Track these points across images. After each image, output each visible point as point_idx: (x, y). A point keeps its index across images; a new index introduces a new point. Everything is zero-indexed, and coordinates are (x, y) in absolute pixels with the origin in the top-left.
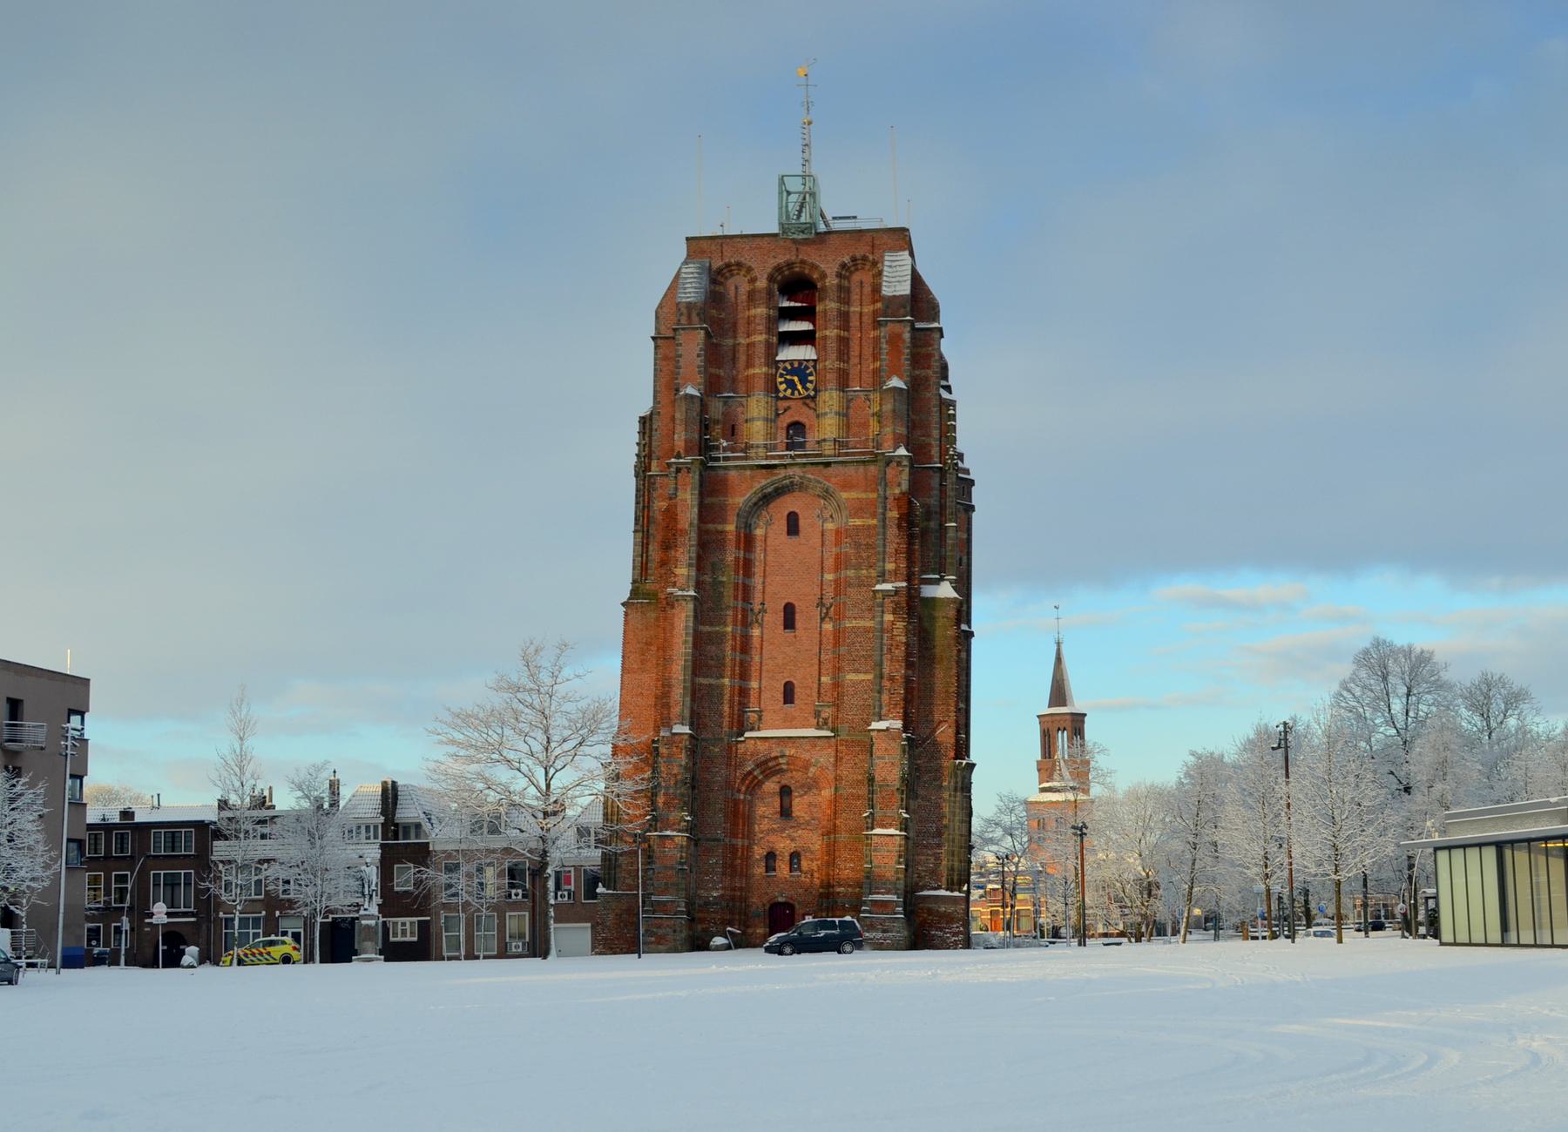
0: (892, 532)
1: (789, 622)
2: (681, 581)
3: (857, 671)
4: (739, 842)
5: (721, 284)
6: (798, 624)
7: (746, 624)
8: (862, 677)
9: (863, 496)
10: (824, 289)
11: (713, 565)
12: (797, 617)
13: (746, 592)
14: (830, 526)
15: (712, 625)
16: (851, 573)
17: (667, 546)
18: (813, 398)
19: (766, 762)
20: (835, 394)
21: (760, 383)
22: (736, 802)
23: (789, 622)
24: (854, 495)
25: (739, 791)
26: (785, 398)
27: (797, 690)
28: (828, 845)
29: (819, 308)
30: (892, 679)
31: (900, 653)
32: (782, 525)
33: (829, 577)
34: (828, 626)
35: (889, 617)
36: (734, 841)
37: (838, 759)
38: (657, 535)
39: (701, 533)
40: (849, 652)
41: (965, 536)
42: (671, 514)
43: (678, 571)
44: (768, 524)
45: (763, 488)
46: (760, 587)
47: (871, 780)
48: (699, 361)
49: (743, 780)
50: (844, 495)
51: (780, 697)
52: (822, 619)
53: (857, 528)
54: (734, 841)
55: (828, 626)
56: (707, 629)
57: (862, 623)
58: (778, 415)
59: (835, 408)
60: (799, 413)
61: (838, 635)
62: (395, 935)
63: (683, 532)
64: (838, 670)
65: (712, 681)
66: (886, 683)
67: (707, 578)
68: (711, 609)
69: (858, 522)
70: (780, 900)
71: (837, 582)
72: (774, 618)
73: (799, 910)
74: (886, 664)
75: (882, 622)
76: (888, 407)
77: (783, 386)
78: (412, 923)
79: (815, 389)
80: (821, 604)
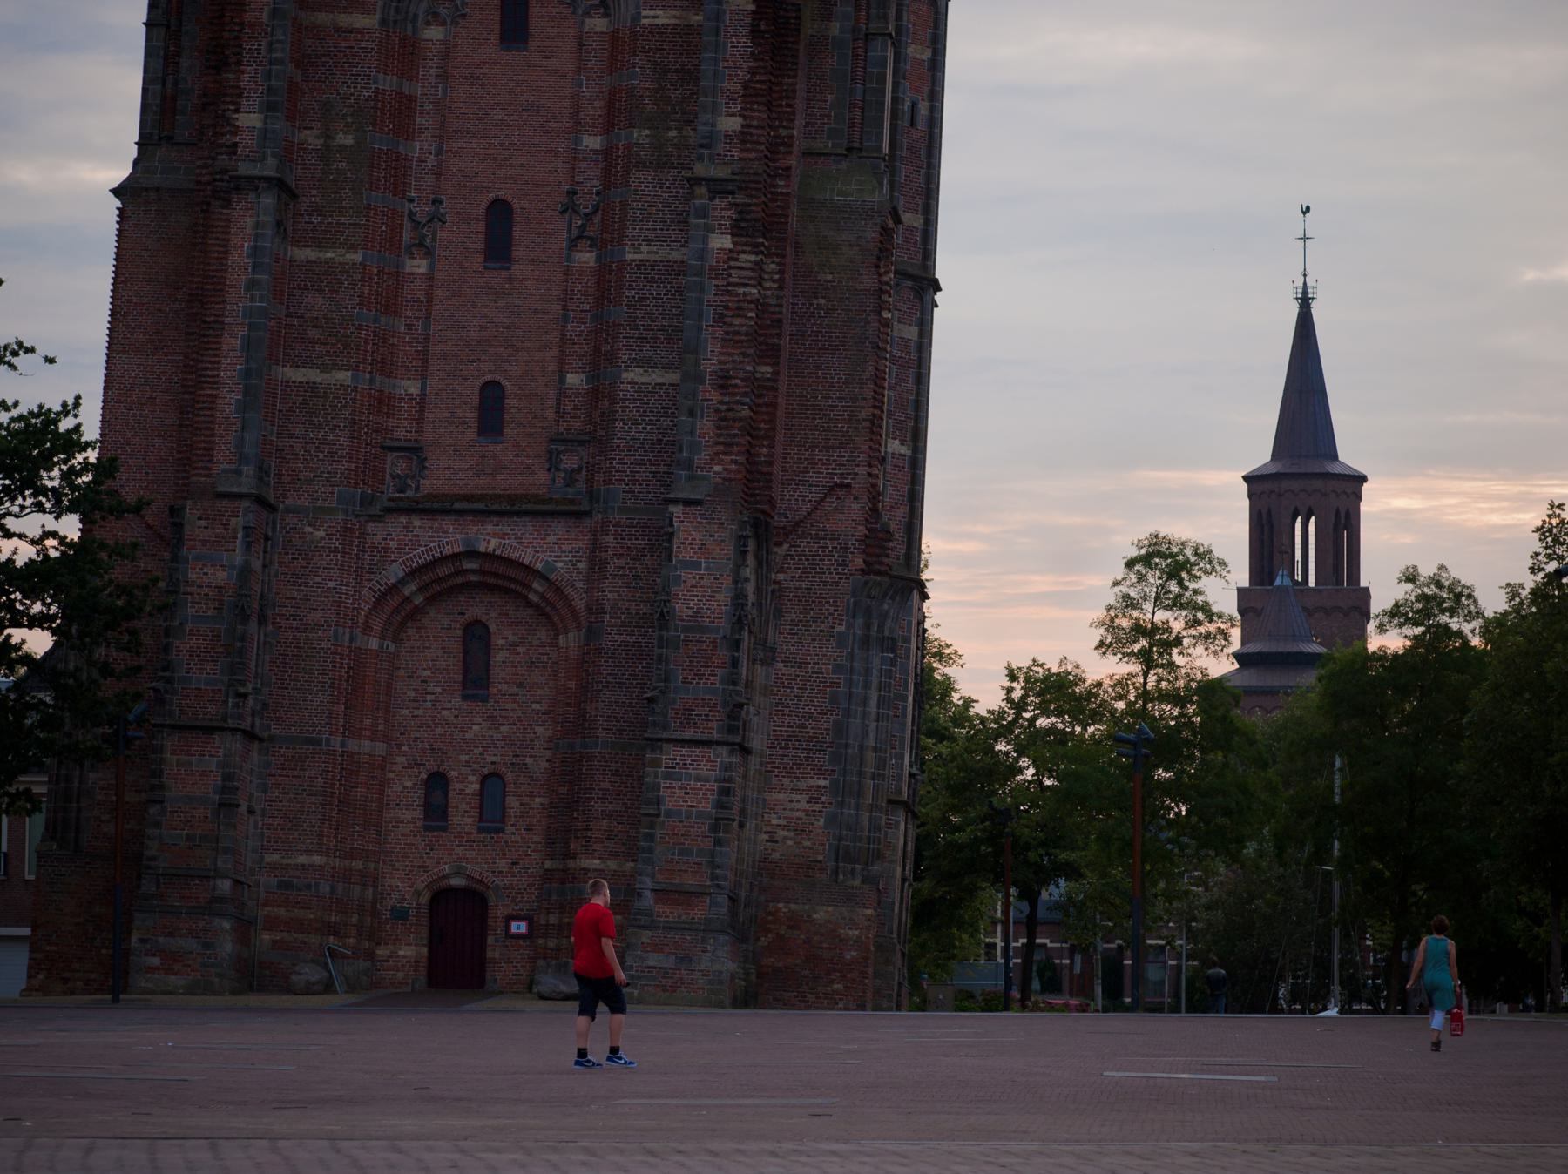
0: (738, 43)
1: (498, 248)
2: (247, 142)
3: (648, 364)
4: (363, 747)
6: (519, 251)
8: (657, 377)
12: (517, 232)
14: (599, 24)
15: (320, 246)
16: (641, 135)
23: (498, 248)
25: (367, 629)
27: (511, 403)
30: (723, 384)
33: (592, 142)
34: (586, 258)
35: (726, 242)
36: (352, 745)
37: (597, 566)
41: (927, 55)
46: (431, 161)
49: (379, 602)
51: (470, 416)
52: (573, 244)
53: (658, 31)
54: (352, 745)
55: (586, 258)
56: (310, 254)
61: (607, 279)
64: (601, 363)
65: (314, 376)
67: (312, 138)
70: (457, 882)
71: (608, 153)
73: (498, 909)
75: (702, 254)
80: (569, 208)
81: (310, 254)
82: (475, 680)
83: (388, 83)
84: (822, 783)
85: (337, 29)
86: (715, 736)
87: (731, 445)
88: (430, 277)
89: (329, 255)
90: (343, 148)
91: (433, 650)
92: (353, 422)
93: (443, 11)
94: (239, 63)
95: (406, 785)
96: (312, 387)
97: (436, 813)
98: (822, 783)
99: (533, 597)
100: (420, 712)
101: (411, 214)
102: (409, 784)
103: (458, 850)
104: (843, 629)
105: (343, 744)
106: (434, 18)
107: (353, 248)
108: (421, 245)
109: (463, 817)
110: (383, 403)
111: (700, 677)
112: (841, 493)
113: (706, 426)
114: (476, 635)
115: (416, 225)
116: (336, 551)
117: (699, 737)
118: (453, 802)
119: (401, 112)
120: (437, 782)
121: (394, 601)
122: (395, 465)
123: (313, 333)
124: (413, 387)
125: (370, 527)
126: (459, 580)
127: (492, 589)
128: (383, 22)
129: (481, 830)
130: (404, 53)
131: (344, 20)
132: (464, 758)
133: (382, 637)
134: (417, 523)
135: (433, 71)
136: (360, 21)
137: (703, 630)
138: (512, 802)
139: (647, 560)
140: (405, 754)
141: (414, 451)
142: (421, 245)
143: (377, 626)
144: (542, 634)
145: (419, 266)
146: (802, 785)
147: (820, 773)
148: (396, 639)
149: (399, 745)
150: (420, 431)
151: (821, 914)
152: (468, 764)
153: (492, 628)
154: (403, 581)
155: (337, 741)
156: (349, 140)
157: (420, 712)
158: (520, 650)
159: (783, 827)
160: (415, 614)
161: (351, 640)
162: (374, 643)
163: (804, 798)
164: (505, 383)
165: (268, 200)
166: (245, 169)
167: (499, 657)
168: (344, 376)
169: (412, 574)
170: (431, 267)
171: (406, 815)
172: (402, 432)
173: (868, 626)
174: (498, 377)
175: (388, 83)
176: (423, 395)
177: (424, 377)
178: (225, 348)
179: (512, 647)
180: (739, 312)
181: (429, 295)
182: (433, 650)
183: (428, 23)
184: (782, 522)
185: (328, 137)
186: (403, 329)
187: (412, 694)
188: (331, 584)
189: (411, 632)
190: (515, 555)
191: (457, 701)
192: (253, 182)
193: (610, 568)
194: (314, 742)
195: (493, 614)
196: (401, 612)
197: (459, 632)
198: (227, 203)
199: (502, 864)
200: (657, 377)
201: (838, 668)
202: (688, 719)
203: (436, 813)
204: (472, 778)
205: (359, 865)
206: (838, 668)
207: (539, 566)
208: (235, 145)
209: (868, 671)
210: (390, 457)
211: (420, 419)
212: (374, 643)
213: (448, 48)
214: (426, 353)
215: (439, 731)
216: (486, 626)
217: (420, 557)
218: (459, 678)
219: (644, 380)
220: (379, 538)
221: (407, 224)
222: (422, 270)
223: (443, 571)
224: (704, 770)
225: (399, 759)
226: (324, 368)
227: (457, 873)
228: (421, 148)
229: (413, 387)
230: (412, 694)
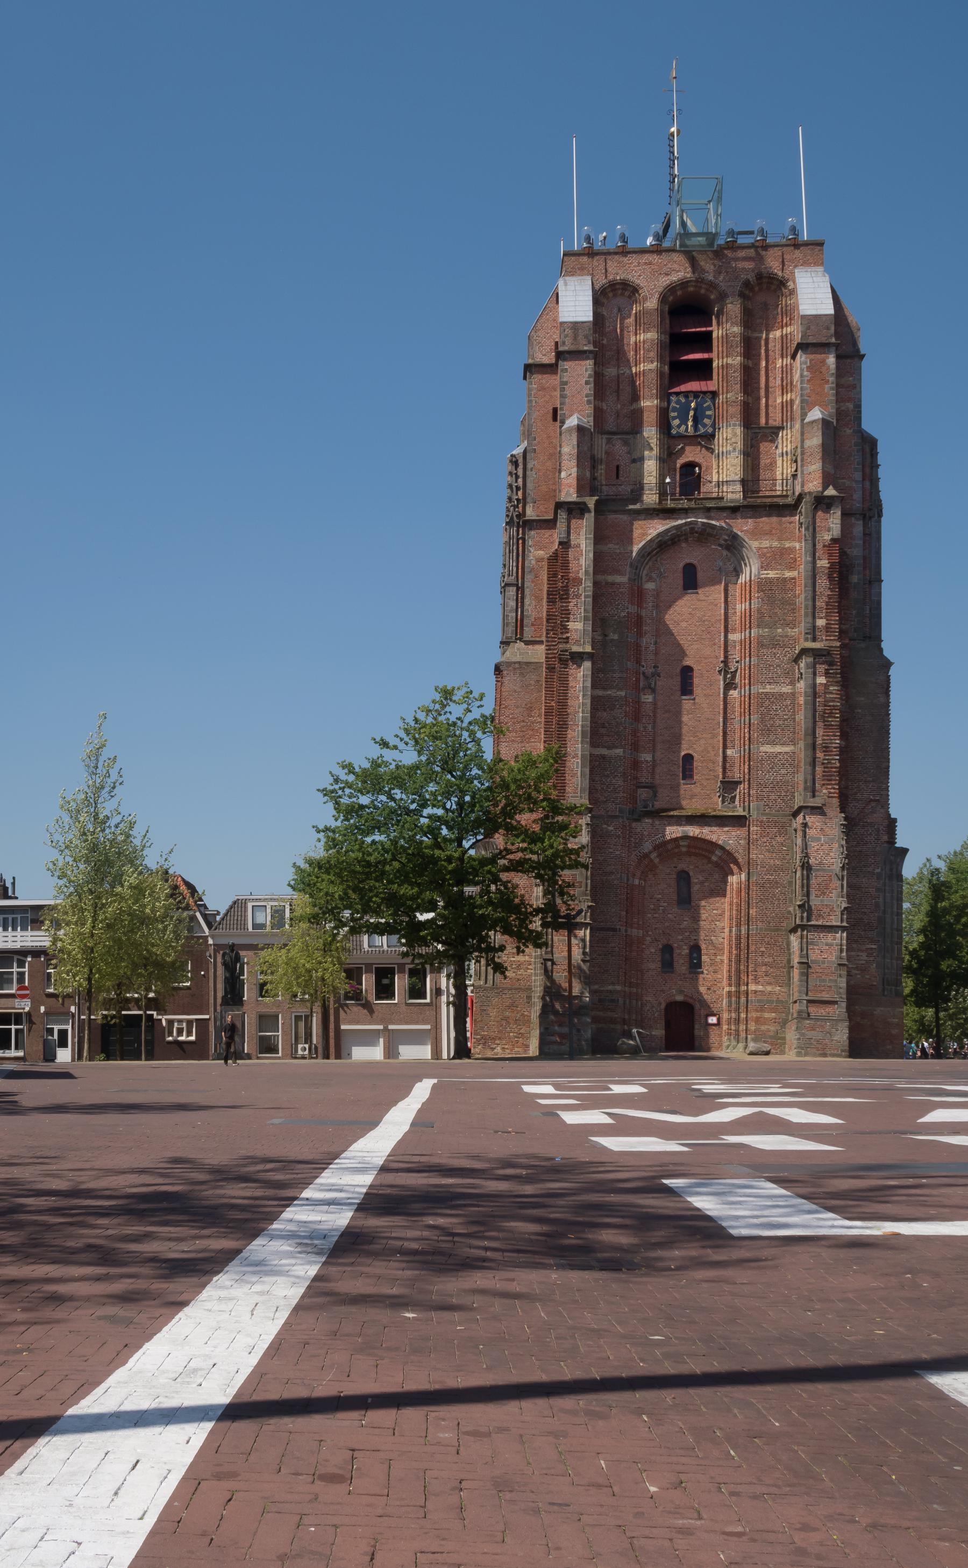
2: (573, 636)
4: (635, 932)
6: (697, 690)
9: (775, 544)
15: (604, 689)
17: (559, 594)
18: (713, 436)
20: (739, 430)
24: (766, 544)
26: (681, 437)
28: (739, 938)
29: (717, 333)
31: (835, 721)
32: (678, 579)
35: (821, 680)
38: (538, 585)
39: (595, 584)
42: (559, 562)
43: (571, 625)
46: (652, 647)
47: (806, 867)
48: (589, 390)
50: (754, 544)
59: (739, 446)
60: (691, 454)
62: (171, 1034)
63: (578, 581)
76: (815, 441)
77: (677, 422)
78: (189, 1022)
79: (714, 425)
83: (633, 609)
84: (873, 947)
85: (607, 583)
86: (834, 924)
87: (830, 780)
88: (655, 703)
89: (609, 692)
90: (612, 640)
92: (624, 774)
93: (654, 576)
94: (568, 598)
95: (652, 951)
96: (603, 757)
98: (873, 947)
99: (714, 858)
100: (656, 915)
101: (644, 673)
102: (653, 950)
103: (680, 983)
104: (879, 870)
105: (626, 931)
106: (650, 579)
107: (620, 689)
108: (650, 688)
110: (636, 764)
111: (824, 894)
112: (873, 804)
114: (684, 878)
115: (647, 678)
116: (619, 837)
117: (825, 923)
118: (675, 959)
120: (668, 950)
122: (643, 794)
123: (603, 731)
124: (648, 757)
125: (634, 825)
126: (676, 850)
127: (696, 855)
128: (629, 579)
129: (690, 973)
130: (638, 595)
131: (610, 578)
132: (680, 937)
133: (640, 879)
134: (657, 822)
135: (650, 604)
136: (619, 579)
137: (824, 870)
139: (778, 839)
140: (650, 936)
141: (652, 787)
142: (650, 688)
143: (638, 874)
144: (716, 876)
145: (648, 698)
147: (872, 942)
148: (645, 881)
149: (647, 932)
150: (653, 778)
152: (682, 940)
153: (691, 874)
154: (650, 852)
156: (616, 637)
157: (656, 915)
158: (706, 884)
161: (628, 880)
163: (864, 955)
164: (694, 754)
165: (587, 664)
166: (575, 649)
168: (619, 751)
170: (654, 698)
171: (653, 966)
172: (644, 778)
174: (690, 752)
175: (633, 609)
176: (654, 761)
177: (653, 750)
178: (569, 736)
179: (702, 883)
181: (655, 712)
183: (647, 581)
185: (606, 636)
186: (642, 729)
187: (652, 906)
188: (618, 853)
189: (650, 876)
190: (708, 838)
191: (675, 909)
192: (578, 658)
193: (759, 842)
194: (614, 930)
195: (691, 867)
197: (675, 876)
198: (566, 666)
201: (878, 890)
202: (820, 915)
203: (668, 965)
204: (685, 947)
205: (634, 990)
206: (878, 890)
207: (720, 842)
208: (568, 638)
210: (640, 791)
211: (653, 773)
212: (637, 882)
214: (654, 740)
215: (667, 924)
216: (688, 874)
218: (676, 898)
219: (772, 750)
220: (639, 830)
221: (642, 677)
222: (650, 700)
225: (648, 938)
226: (609, 748)
228: (647, 641)
229: (648, 757)
230: (652, 906)
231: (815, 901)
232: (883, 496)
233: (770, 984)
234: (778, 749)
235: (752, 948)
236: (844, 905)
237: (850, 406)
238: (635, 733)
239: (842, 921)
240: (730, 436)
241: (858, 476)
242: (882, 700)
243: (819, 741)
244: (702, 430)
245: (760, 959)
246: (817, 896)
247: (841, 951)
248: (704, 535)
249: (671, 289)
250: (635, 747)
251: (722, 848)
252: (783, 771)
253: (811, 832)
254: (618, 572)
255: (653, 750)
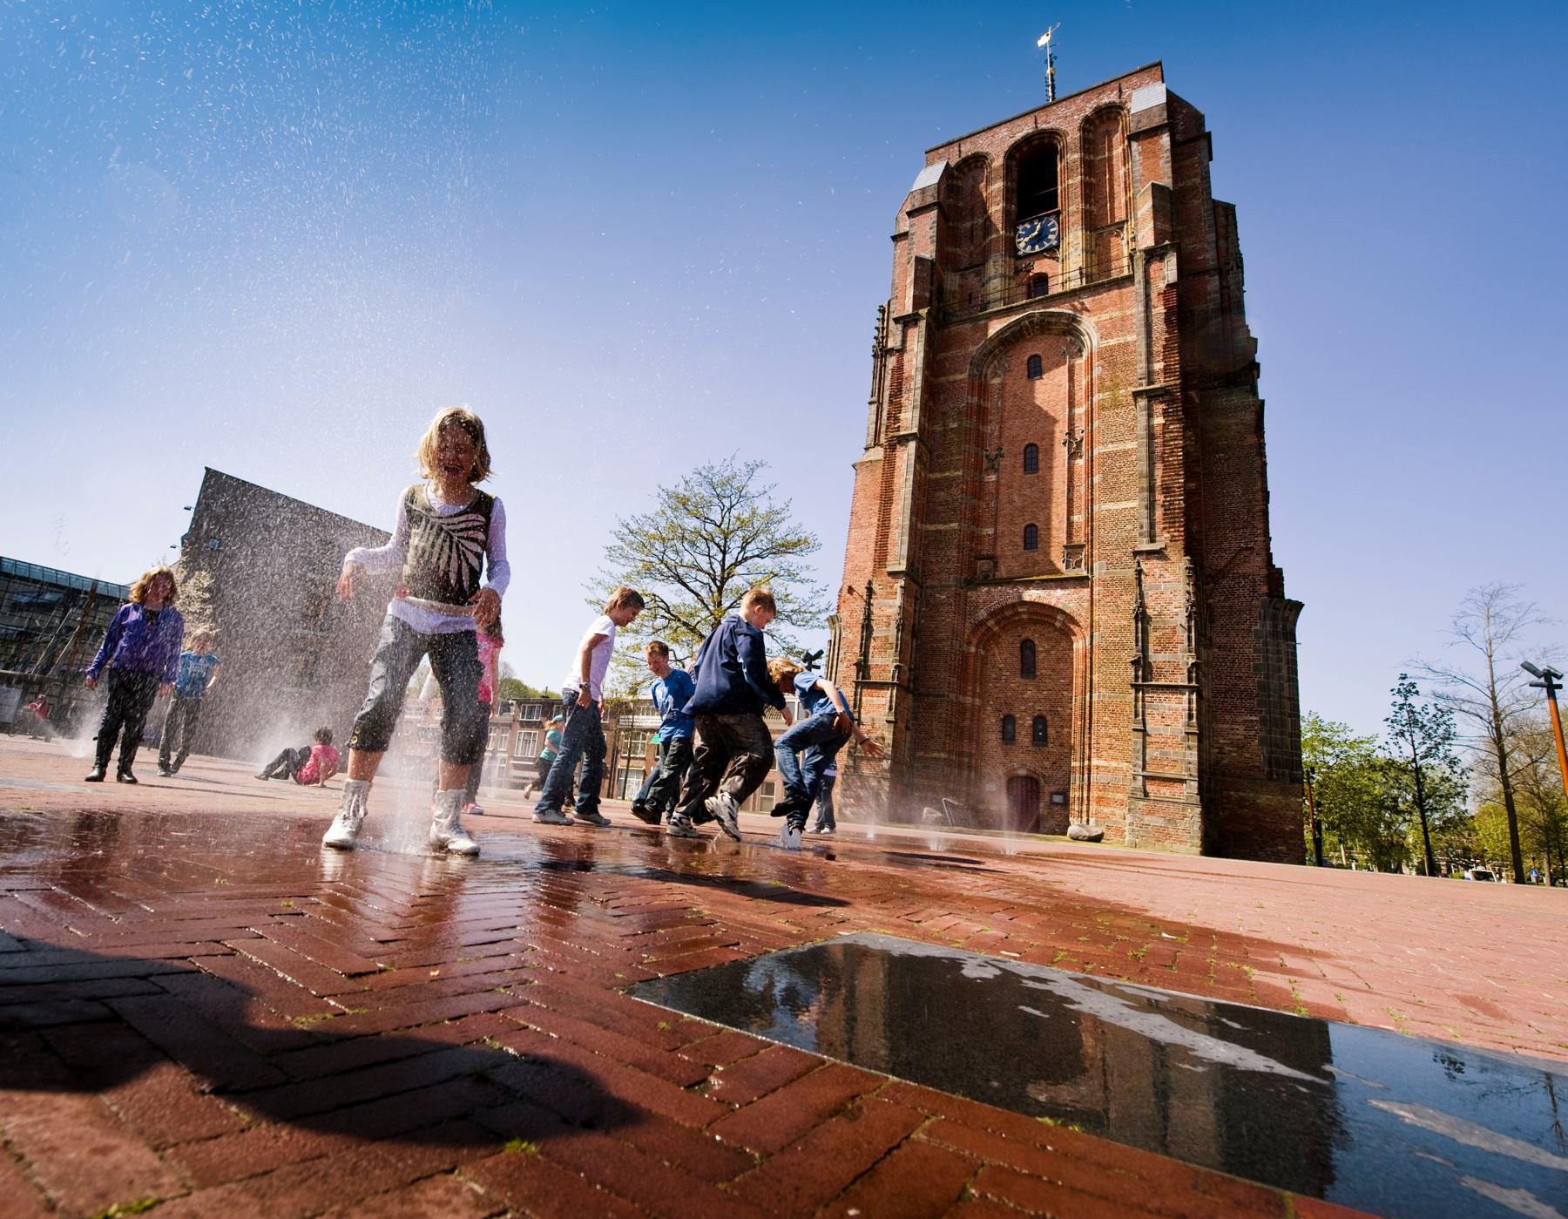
5: (958, 178)
7: (978, 469)
9: (1116, 314)
10: (1066, 147)
11: (944, 413)
13: (980, 440)
15: (942, 471)
17: (897, 392)
18: (1058, 247)
19: (1003, 609)
21: (1001, 246)
22: (965, 657)
25: (969, 643)
26: (1027, 256)
30: (1167, 490)
36: (961, 698)
40: (1104, 480)
43: (902, 416)
44: (1007, 371)
45: (1002, 331)
49: (974, 632)
51: (1020, 541)
53: (1111, 349)
54: (961, 698)
56: (938, 475)
57: (1121, 447)
58: (1017, 271)
65: (942, 527)
66: (1160, 498)
68: (941, 456)
69: (1112, 342)
72: (1012, 463)
74: (1159, 473)
79: (1058, 239)
81: (938, 475)
82: (1028, 668)
86: (1181, 680)
88: (998, 482)
91: (1004, 655)
96: (939, 531)
97: (1008, 738)
99: (1058, 624)
106: (996, 375)
109: (1024, 737)
110: (975, 538)
113: (1159, 513)
114: (1027, 647)
119: (981, 414)
121: (983, 630)
122: (984, 565)
124: (990, 531)
130: (982, 389)
138: (1051, 731)
143: (975, 641)
145: (993, 477)
146: (1239, 719)
147: (1252, 713)
151: (1263, 799)
155: (952, 696)
159: (1231, 744)
160: (994, 637)
162: (973, 649)
163: (1241, 729)
165: (912, 445)
167: (1041, 656)
168: (955, 525)
169: (992, 615)
173: (1275, 626)
177: (995, 525)
179: (1047, 651)
180: (1171, 454)
181: (997, 491)
182: (1004, 655)
184: (1209, 571)
196: (987, 638)
199: (1047, 764)
200: (1123, 505)
209: (1278, 652)
210: (980, 563)
211: (994, 546)
213: (1003, 385)
217: (995, 605)
223: (1007, 613)
224: (1174, 705)
227: (1023, 766)
228: (992, 428)
231: (1156, 658)
232: (1244, 247)
233: (1113, 759)
234: (1123, 505)
235: (1095, 717)
236: (1191, 661)
237: (1198, 180)
238: (974, 509)
239: (1190, 680)
240: (1074, 241)
241: (1212, 237)
242: (1252, 440)
243: (1159, 483)
244: (1047, 245)
245: (1103, 731)
246: (1156, 651)
247: (1190, 717)
248: (1045, 325)
249: (1016, 147)
250: (976, 521)
251: (1063, 612)
252: (1129, 527)
253: (1147, 582)
254: (956, 371)
255: (995, 525)
